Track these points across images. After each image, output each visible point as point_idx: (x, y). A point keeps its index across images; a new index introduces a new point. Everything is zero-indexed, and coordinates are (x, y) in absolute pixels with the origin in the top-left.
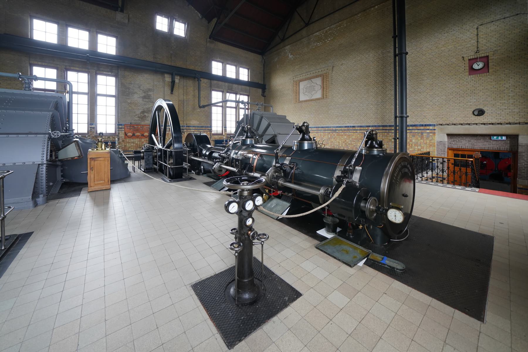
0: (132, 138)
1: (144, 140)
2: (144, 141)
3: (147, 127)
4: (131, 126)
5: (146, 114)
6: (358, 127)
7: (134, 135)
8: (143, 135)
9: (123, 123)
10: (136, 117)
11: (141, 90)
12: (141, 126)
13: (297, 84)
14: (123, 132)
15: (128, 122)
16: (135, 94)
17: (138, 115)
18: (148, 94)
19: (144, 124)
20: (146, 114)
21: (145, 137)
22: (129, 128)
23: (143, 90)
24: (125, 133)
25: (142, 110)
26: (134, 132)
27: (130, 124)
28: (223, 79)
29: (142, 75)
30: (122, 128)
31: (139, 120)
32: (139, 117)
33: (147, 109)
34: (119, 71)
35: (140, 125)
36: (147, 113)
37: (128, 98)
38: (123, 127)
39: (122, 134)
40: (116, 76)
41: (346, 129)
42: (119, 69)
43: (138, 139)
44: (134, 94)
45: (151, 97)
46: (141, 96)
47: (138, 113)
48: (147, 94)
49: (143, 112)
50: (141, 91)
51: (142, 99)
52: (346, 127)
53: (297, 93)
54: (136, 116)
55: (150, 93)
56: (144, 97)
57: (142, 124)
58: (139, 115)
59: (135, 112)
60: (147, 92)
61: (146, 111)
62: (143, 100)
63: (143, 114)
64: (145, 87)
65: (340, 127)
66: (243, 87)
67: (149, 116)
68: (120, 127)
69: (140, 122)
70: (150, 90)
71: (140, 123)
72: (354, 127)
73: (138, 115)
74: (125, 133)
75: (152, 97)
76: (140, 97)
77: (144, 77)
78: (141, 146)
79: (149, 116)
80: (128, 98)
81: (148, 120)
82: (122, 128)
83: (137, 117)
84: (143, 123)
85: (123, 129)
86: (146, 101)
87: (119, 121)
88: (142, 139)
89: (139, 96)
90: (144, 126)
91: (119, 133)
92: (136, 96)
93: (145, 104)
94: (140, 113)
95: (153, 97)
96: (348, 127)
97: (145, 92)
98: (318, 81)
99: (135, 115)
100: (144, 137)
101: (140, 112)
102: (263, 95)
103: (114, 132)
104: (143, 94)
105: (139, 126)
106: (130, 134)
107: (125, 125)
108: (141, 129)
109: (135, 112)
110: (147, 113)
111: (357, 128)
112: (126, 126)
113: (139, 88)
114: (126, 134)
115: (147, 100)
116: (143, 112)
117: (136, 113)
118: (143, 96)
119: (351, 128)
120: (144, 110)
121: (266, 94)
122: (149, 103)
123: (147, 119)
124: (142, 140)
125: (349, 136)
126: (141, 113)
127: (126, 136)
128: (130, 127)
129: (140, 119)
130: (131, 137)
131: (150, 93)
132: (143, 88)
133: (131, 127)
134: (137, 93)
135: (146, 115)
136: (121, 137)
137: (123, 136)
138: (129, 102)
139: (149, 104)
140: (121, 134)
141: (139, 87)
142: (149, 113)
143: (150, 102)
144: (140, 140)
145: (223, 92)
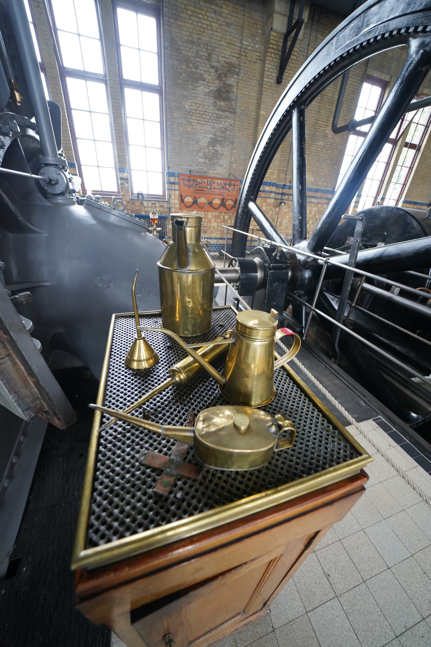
0: (191, 209)
1: (212, 216)
2: (211, 219)
3: (219, 183)
4: (191, 178)
5: (218, 148)
7: (195, 202)
8: (210, 204)
9: (176, 171)
10: (199, 154)
11: (212, 67)
12: (209, 180)
14: (177, 193)
15: (184, 169)
16: (201, 82)
17: (202, 151)
18: (227, 82)
19: (214, 175)
21: (214, 208)
22: (186, 183)
24: (181, 196)
25: (211, 136)
26: (197, 195)
27: (189, 173)
30: (174, 183)
31: (205, 163)
32: (205, 156)
35: (207, 178)
38: (177, 180)
39: (175, 199)
43: (203, 213)
46: (211, 88)
47: (204, 145)
48: (225, 84)
49: (214, 142)
50: (213, 71)
51: (212, 100)
54: (199, 151)
55: (231, 81)
57: (209, 175)
58: (207, 150)
60: (226, 76)
61: (220, 139)
63: (213, 147)
64: (220, 58)
67: (223, 154)
68: (172, 179)
71: (206, 172)
73: (202, 151)
74: (181, 196)
75: (233, 92)
78: (205, 229)
81: (221, 166)
82: (174, 183)
83: (201, 154)
84: (212, 173)
85: (177, 187)
86: (221, 107)
87: (170, 165)
88: (209, 213)
89: (207, 91)
90: (215, 180)
91: (170, 196)
93: (218, 117)
94: (207, 144)
95: (235, 94)
97: (219, 78)
99: (198, 149)
100: (211, 208)
101: (209, 140)
103: (161, 193)
104: (216, 82)
105: (206, 181)
106: (189, 200)
107: (179, 175)
108: (209, 187)
109: (198, 141)
110: (222, 145)
112: (182, 177)
113: (209, 60)
114: (182, 200)
115: (223, 104)
118: (215, 89)
120: (214, 135)
123: (220, 162)
124: (208, 215)
126: (209, 144)
127: (183, 205)
128: (189, 181)
129: (207, 160)
130: (191, 206)
131: (231, 81)
132: (218, 62)
133: (191, 183)
135: (218, 151)
136: (173, 205)
137: (176, 204)
138: (187, 107)
139: (226, 117)
140: (173, 197)
142: (224, 147)
143: (230, 112)
144: (205, 215)
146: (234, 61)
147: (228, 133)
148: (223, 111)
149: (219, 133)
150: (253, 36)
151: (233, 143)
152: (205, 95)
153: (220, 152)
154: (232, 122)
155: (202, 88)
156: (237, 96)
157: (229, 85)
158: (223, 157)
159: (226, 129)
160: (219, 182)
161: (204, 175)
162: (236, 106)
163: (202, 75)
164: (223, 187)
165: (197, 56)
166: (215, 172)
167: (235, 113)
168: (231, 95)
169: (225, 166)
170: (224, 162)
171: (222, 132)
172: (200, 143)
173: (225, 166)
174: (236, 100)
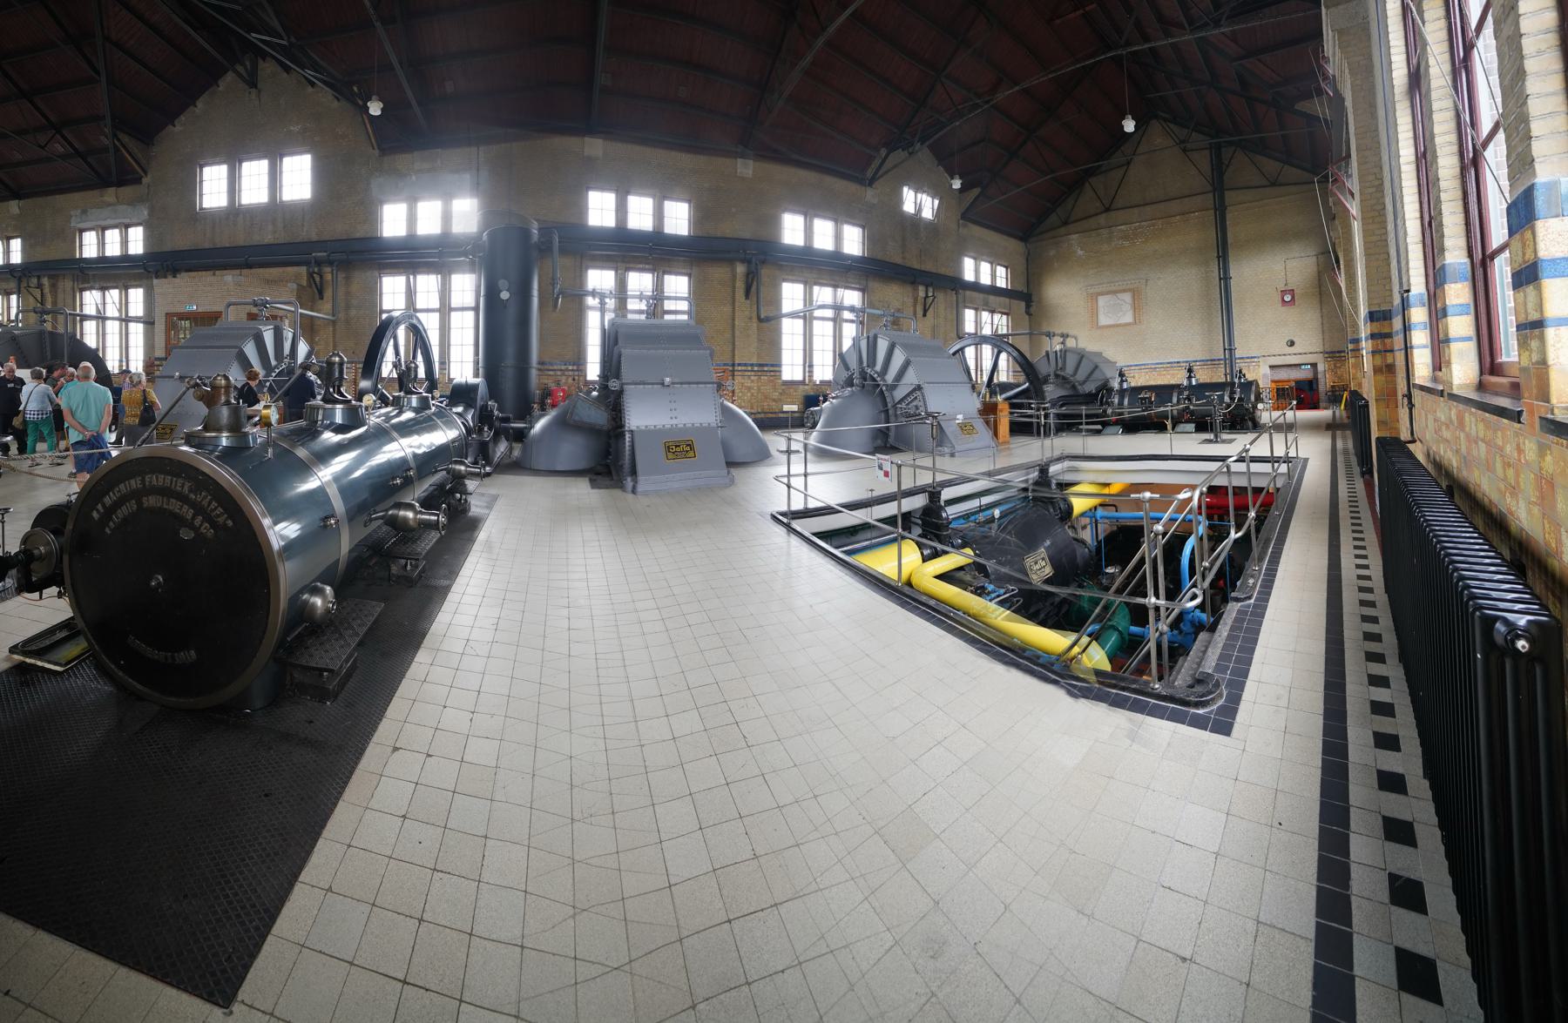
6: (1183, 362)
13: (1094, 298)
28: (976, 287)
41: (1168, 365)
52: (1168, 363)
53: (1094, 313)
65: (1161, 364)
66: (1002, 299)
72: (1178, 362)
96: (1171, 363)
98: (1127, 297)
102: (1028, 313)
111: (1182, 364)
119: (1175, 365)
121: (1032, 310)
125: (1173, 374)
145: (805, 283)
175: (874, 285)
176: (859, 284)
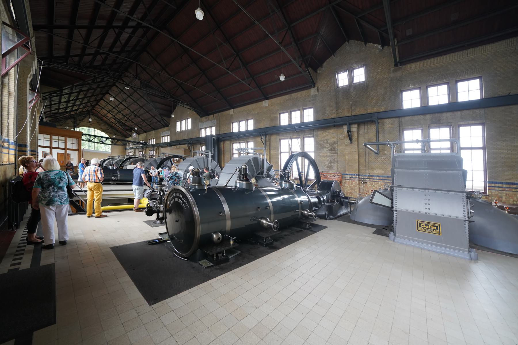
5: (332, 164)
11: (328, 144)
20: (332, 164)
23: (330, 144)
29: (328, 131)
31: (328, 169)
32: (328, 167)
33: (333, 159)
34: (315, 132)
36: (333, 163)
37: (321, 152)
40: (313, 136)
42: (314, 131)
44: (324, 148)
45: (336, 149)
48: (333, 147)
49: (330, 162)
51: (329, 152)
55: (335, 146)
56: (331, 150)
58: (328, 165)
59: (325, 163)
60: (333, 145)
62: (330, 153)
67: (334, 166)
69: (328, 171)
70: (334, 143)
71: (328, 172)
76: (327, 150)
77: (330, 133)
79: (334, 166)
80: (321, 152)
81: (334, 169)
83: (326, 166)
89: (327, 150)
92: (325, 149)
93: (331, 156)
97: (331, 146)
105: (327, 174)
109: (325, 163)
115: (333, 152)
116: (330, 162)
117: (326, 164)
122: (335, 154)
126: (329, 163)
129: (329, 168)
131: (335, 146)
132: (330, 142)
134: (326, 147)
138: (321, 155)
141: (327, 142)
142: (335, 164)
146: (336, 141)
147: (336, 159)
148: (333, 154)
149: (332, 160)
150: (341, 134)
151: (338, 162)
152: (327, 151)
153: (333, 165)
154: (337, 156)
155: (325, 149)
156: (337, 149)
157: (335, 147)
158: (334, 167)
159: (335, 158)
160: (333, 175)
161: (327, 173)
162: (337, 151)
163: (325, 146)
164: (335, 176)
165: (324, 142)
166: (332, 171)
167: (338, 154)
168: (336, 149)
169: (335, 169)
170: (335, 168)
171: (333, 159)
172: (326, 164)
173: (335, 169)
174: (337, 150)
175: (320, 133)
176: (311, 134)
